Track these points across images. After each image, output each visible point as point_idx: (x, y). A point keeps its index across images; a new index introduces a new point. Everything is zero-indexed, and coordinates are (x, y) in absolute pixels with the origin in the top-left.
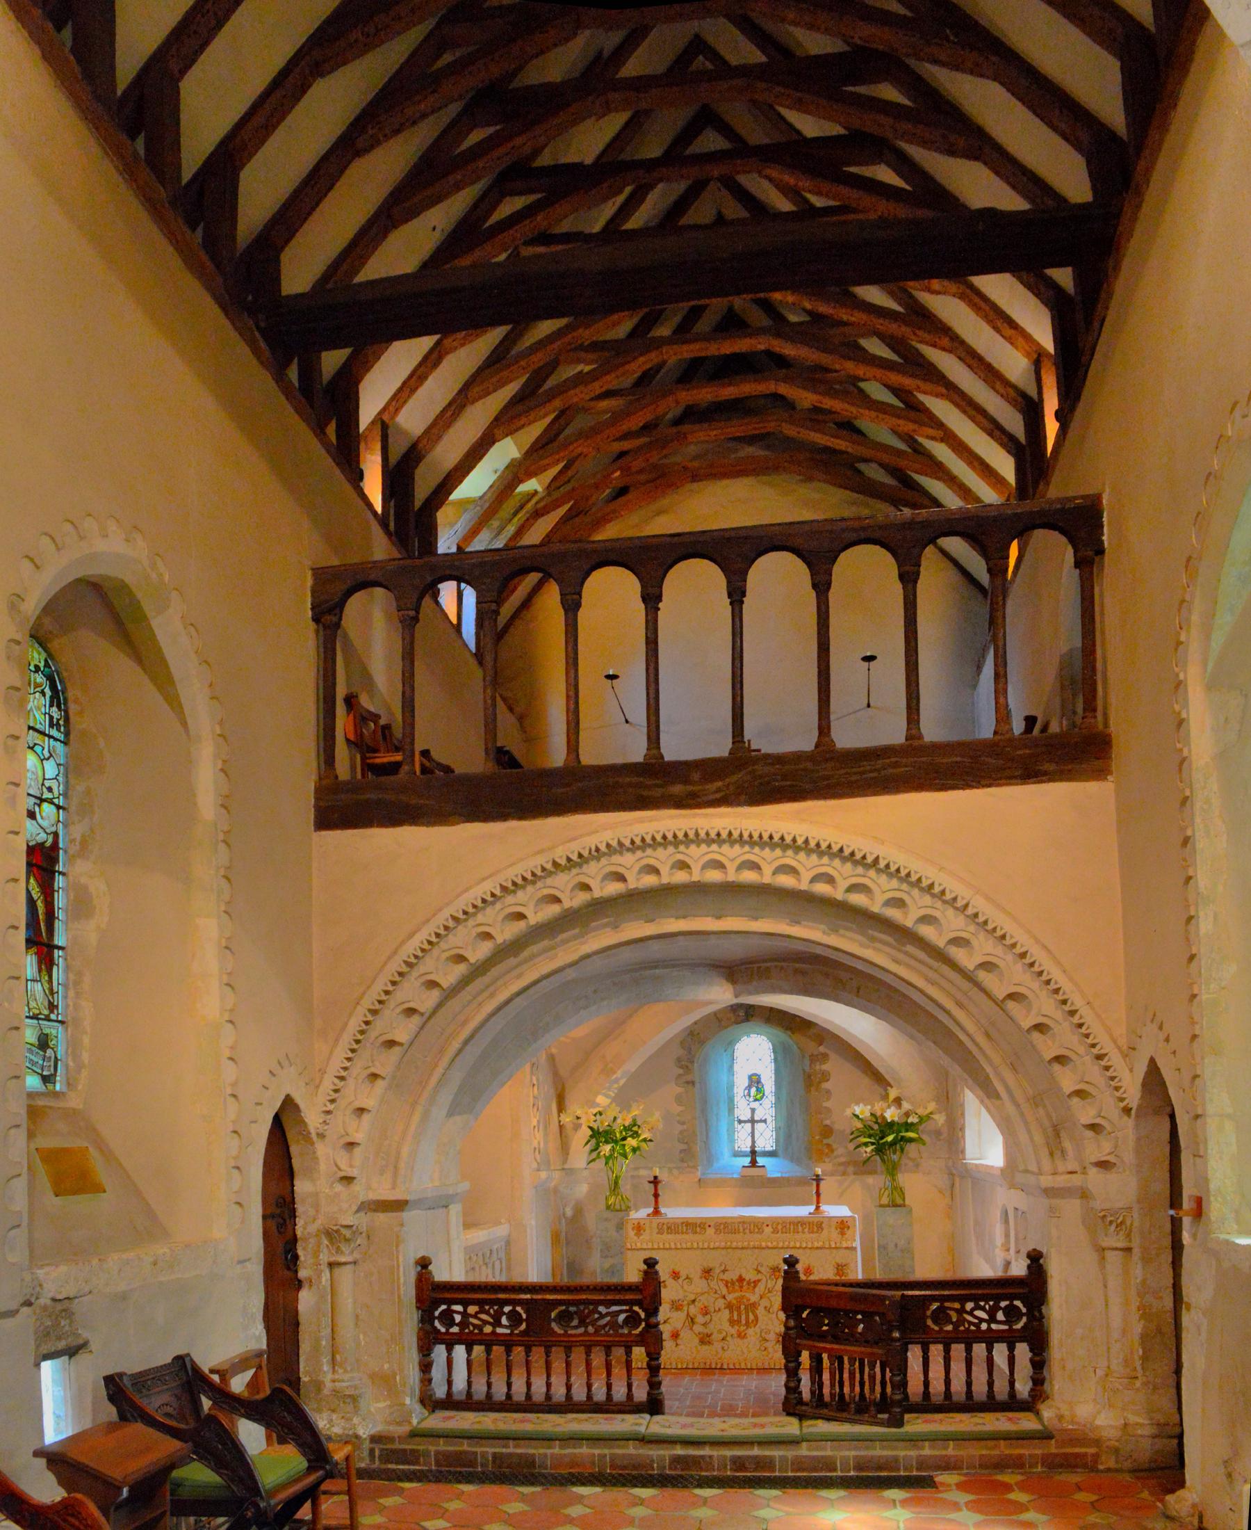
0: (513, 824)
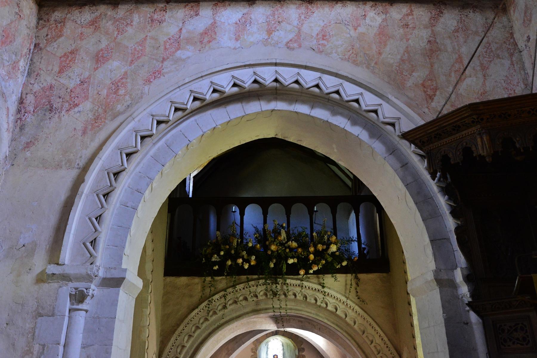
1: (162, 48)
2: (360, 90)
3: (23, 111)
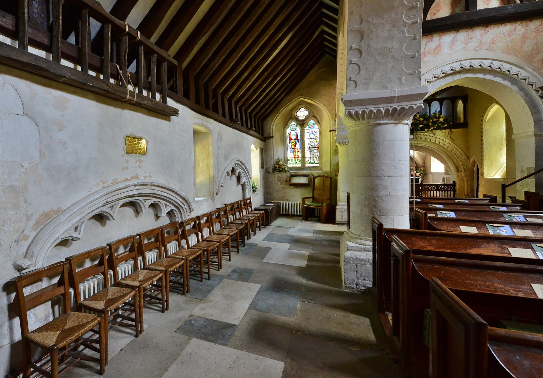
2: (511, 66)
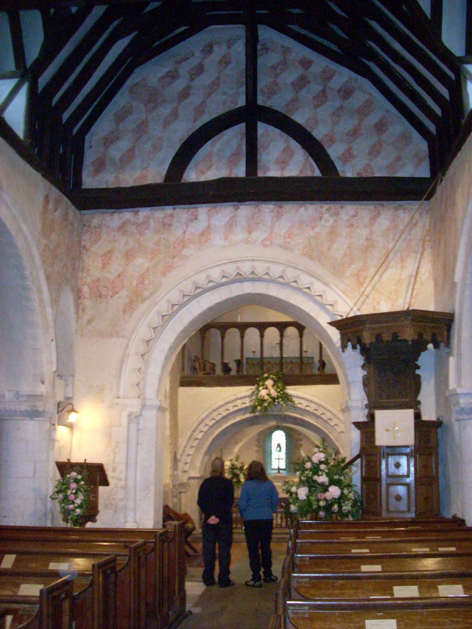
0: (227, 388)
1: (172, 247)
3: (82, 297)
